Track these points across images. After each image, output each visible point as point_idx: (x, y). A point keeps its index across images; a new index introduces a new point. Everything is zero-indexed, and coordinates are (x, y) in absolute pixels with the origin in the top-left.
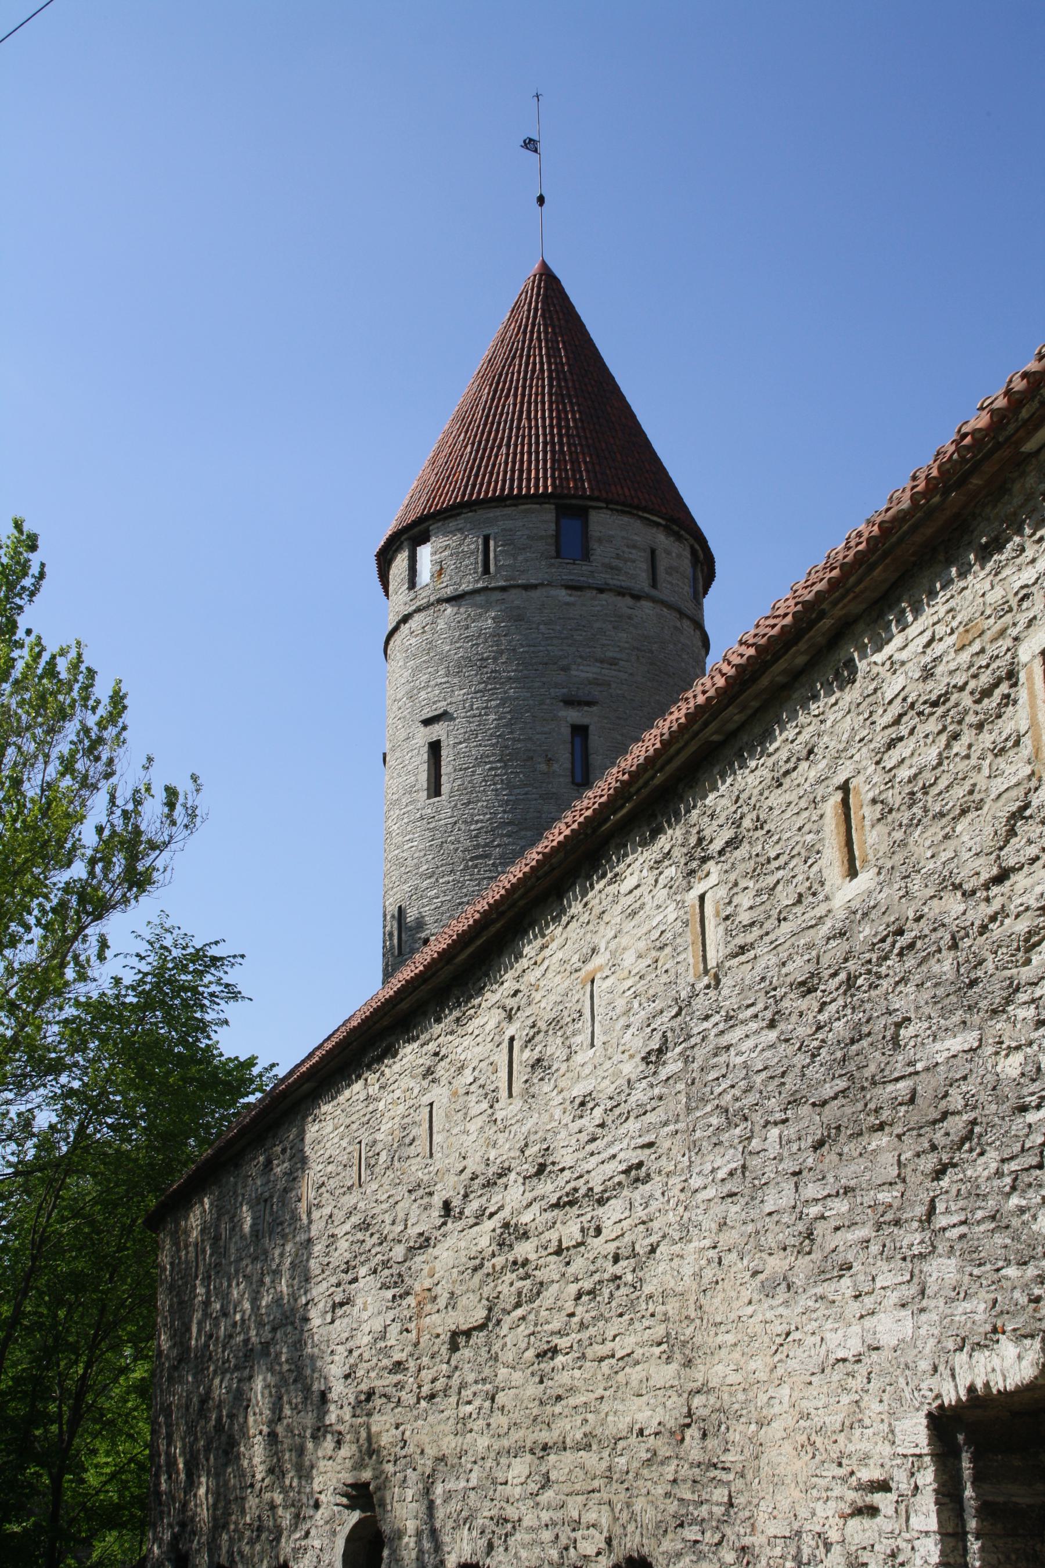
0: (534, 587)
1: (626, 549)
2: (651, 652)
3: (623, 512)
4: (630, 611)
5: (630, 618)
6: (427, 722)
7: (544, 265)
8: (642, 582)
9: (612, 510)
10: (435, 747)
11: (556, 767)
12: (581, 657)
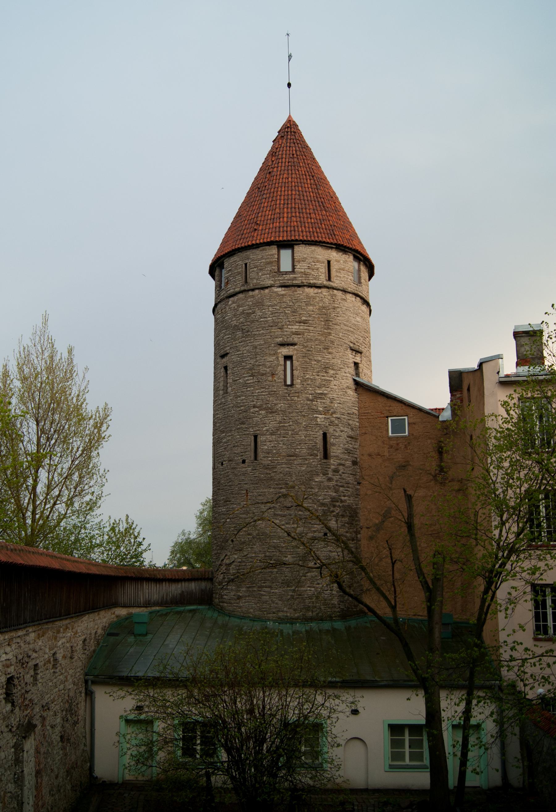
8: (322, 279)
12: (289, 321)
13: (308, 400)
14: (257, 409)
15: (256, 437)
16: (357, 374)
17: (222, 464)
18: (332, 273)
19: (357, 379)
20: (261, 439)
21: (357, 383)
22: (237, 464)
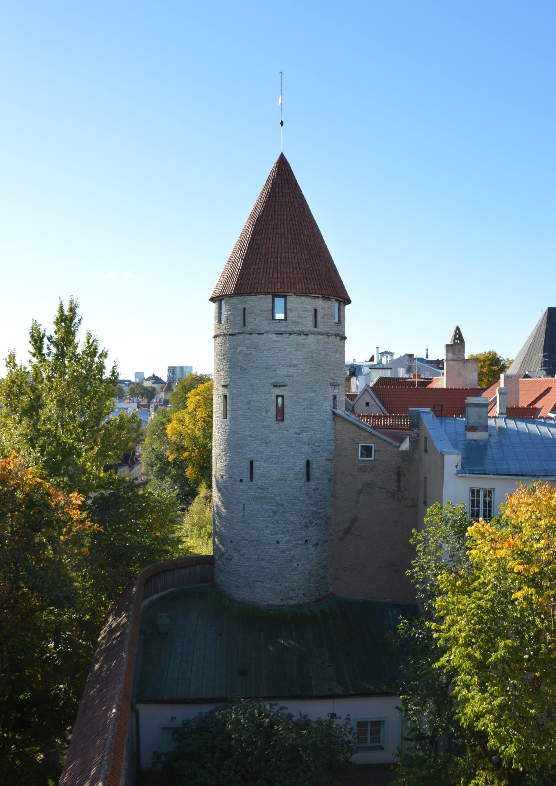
0: (263, 334)
1: (302, 313)
2: (313, 358)
3: (301, 295)
4: (303, 341)
5: (303, 344)
11: (269, 414)
12: (281, 365)
13: (296, 433)
14: (253, 439)
15: (252, 463)
16: (335, 407)
18: (318, 320)
19: (335, 410)
20: (256, 464)
21: (334, 413)
22: (236, 481)
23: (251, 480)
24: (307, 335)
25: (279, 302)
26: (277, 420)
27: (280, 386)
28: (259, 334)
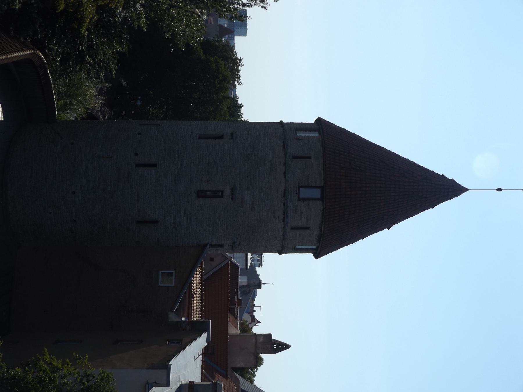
0: (285, 177)
6: (232, 134)
7: (466, 190)
9: (323, 210)
10: (221, 137)
15: (154, 165)
16: (212, 246)
17: (139, 134)
19: (208, 246)
23: (138, 165)
24: (284, 220)
25: (317, 193)
26: (198, 191)
27: (232, 194)
28: (285, 173)
